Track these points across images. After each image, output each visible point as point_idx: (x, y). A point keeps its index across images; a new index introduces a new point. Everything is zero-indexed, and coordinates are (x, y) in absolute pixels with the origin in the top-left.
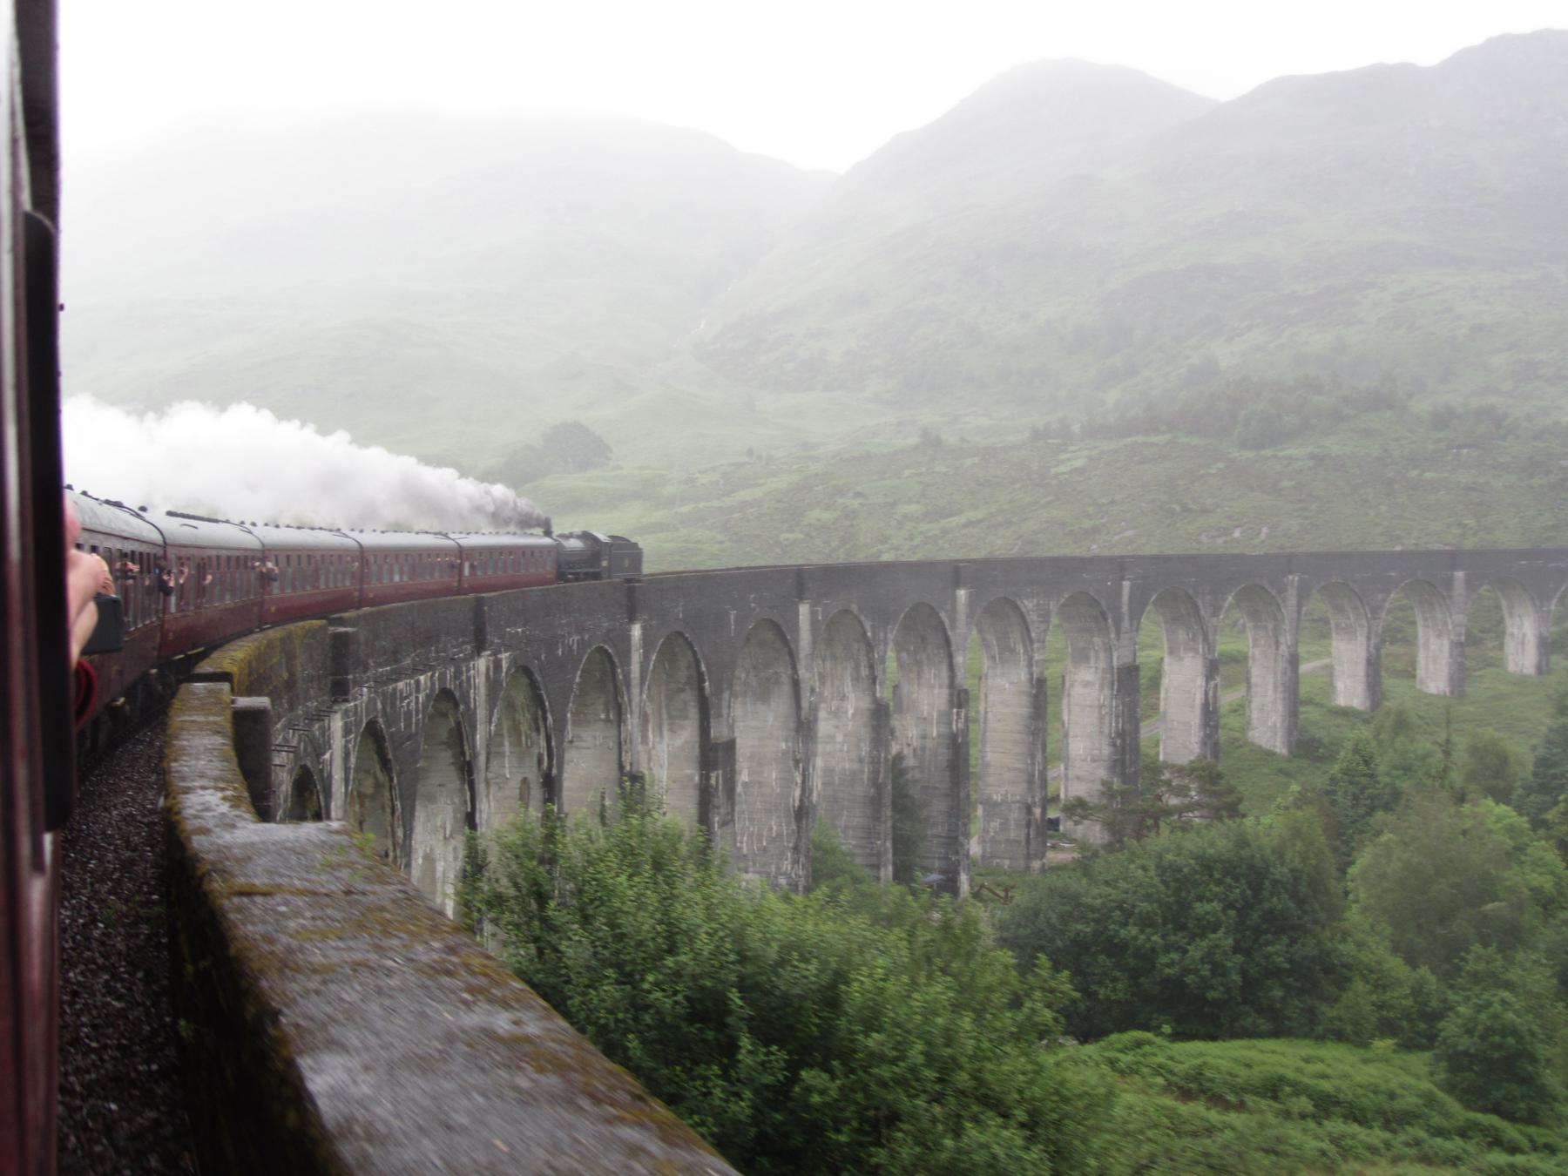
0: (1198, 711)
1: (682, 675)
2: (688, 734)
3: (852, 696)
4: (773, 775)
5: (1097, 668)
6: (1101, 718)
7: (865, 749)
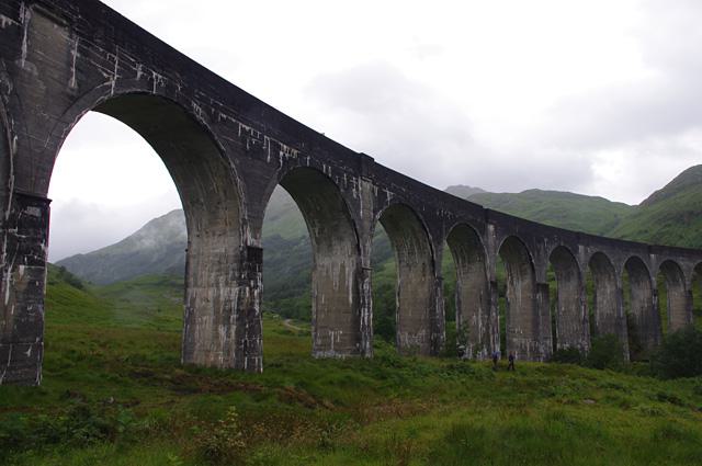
1: (524, 257)
2: (528, 281)
3: (608, 286)
4: (573, 307)
7: (615, 305)
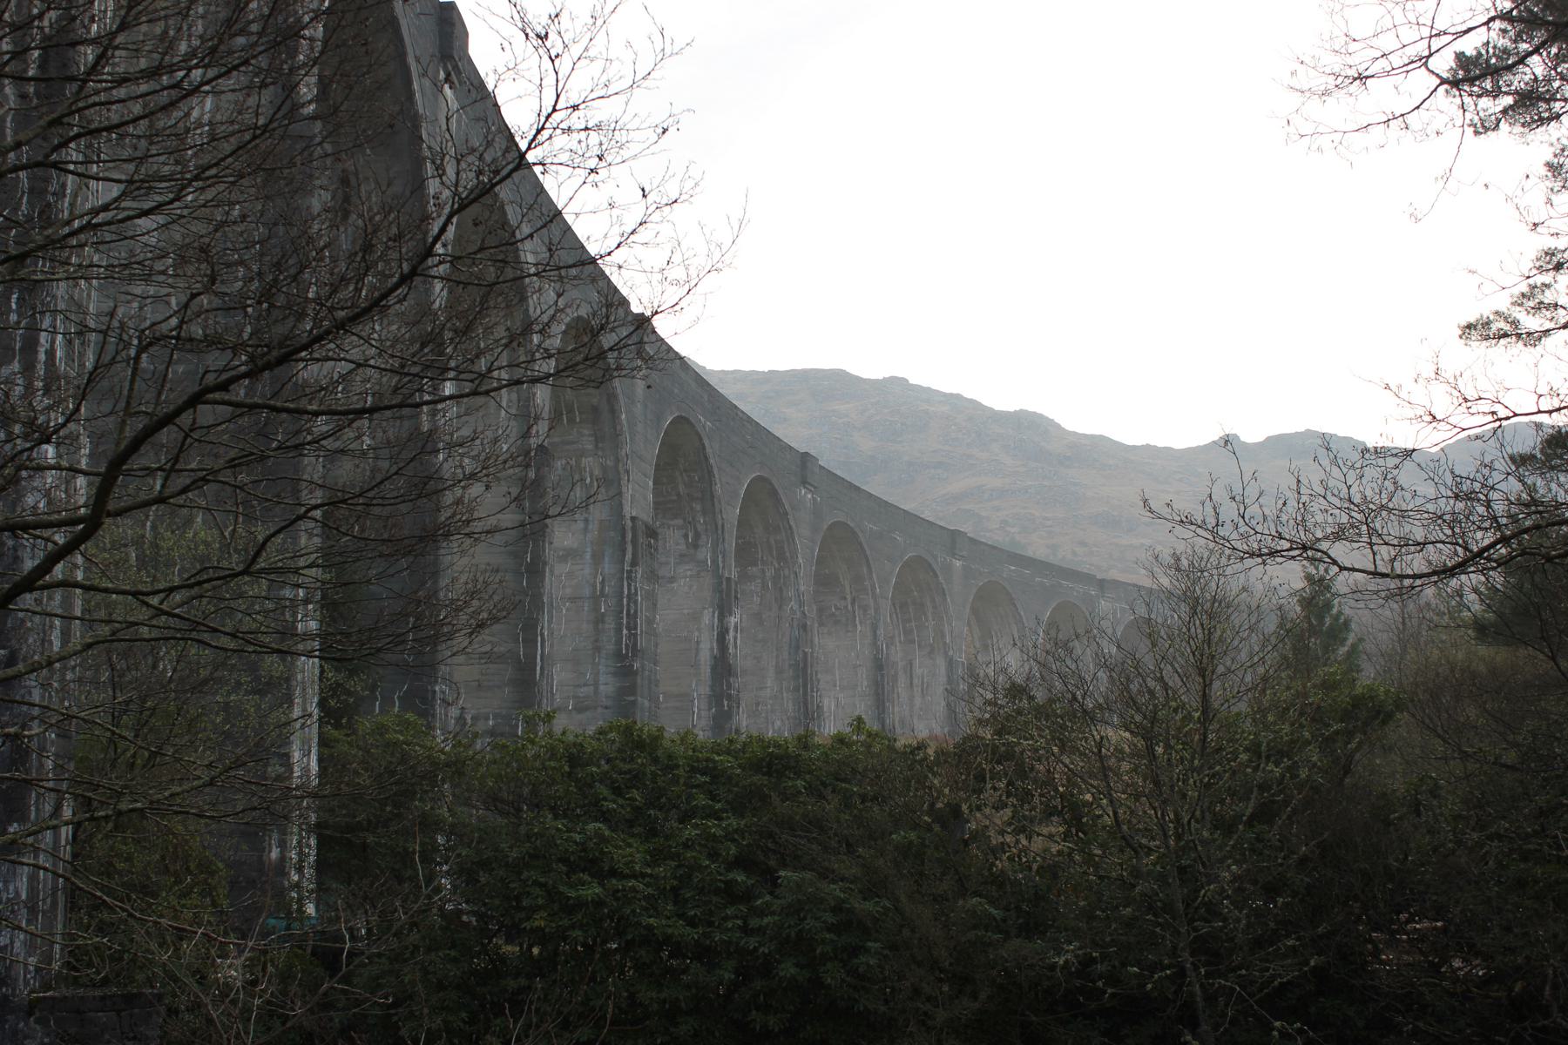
0: (706, 670)
5: (586, 520)
6: (599, 620)
